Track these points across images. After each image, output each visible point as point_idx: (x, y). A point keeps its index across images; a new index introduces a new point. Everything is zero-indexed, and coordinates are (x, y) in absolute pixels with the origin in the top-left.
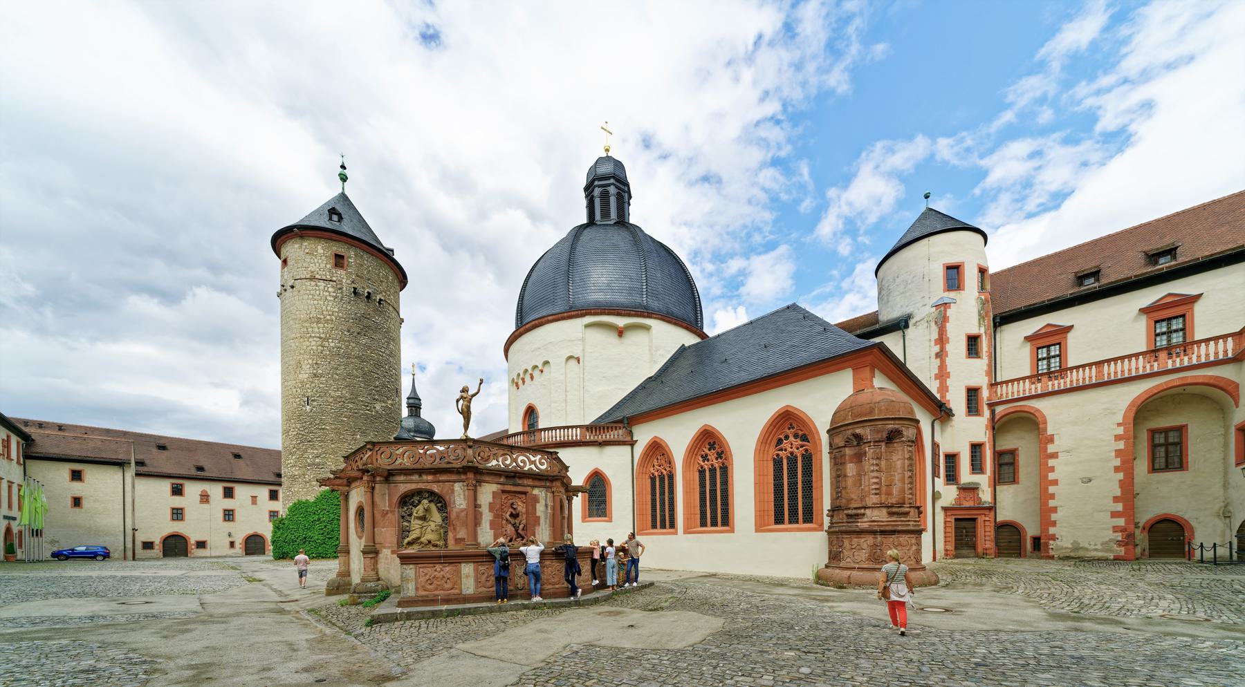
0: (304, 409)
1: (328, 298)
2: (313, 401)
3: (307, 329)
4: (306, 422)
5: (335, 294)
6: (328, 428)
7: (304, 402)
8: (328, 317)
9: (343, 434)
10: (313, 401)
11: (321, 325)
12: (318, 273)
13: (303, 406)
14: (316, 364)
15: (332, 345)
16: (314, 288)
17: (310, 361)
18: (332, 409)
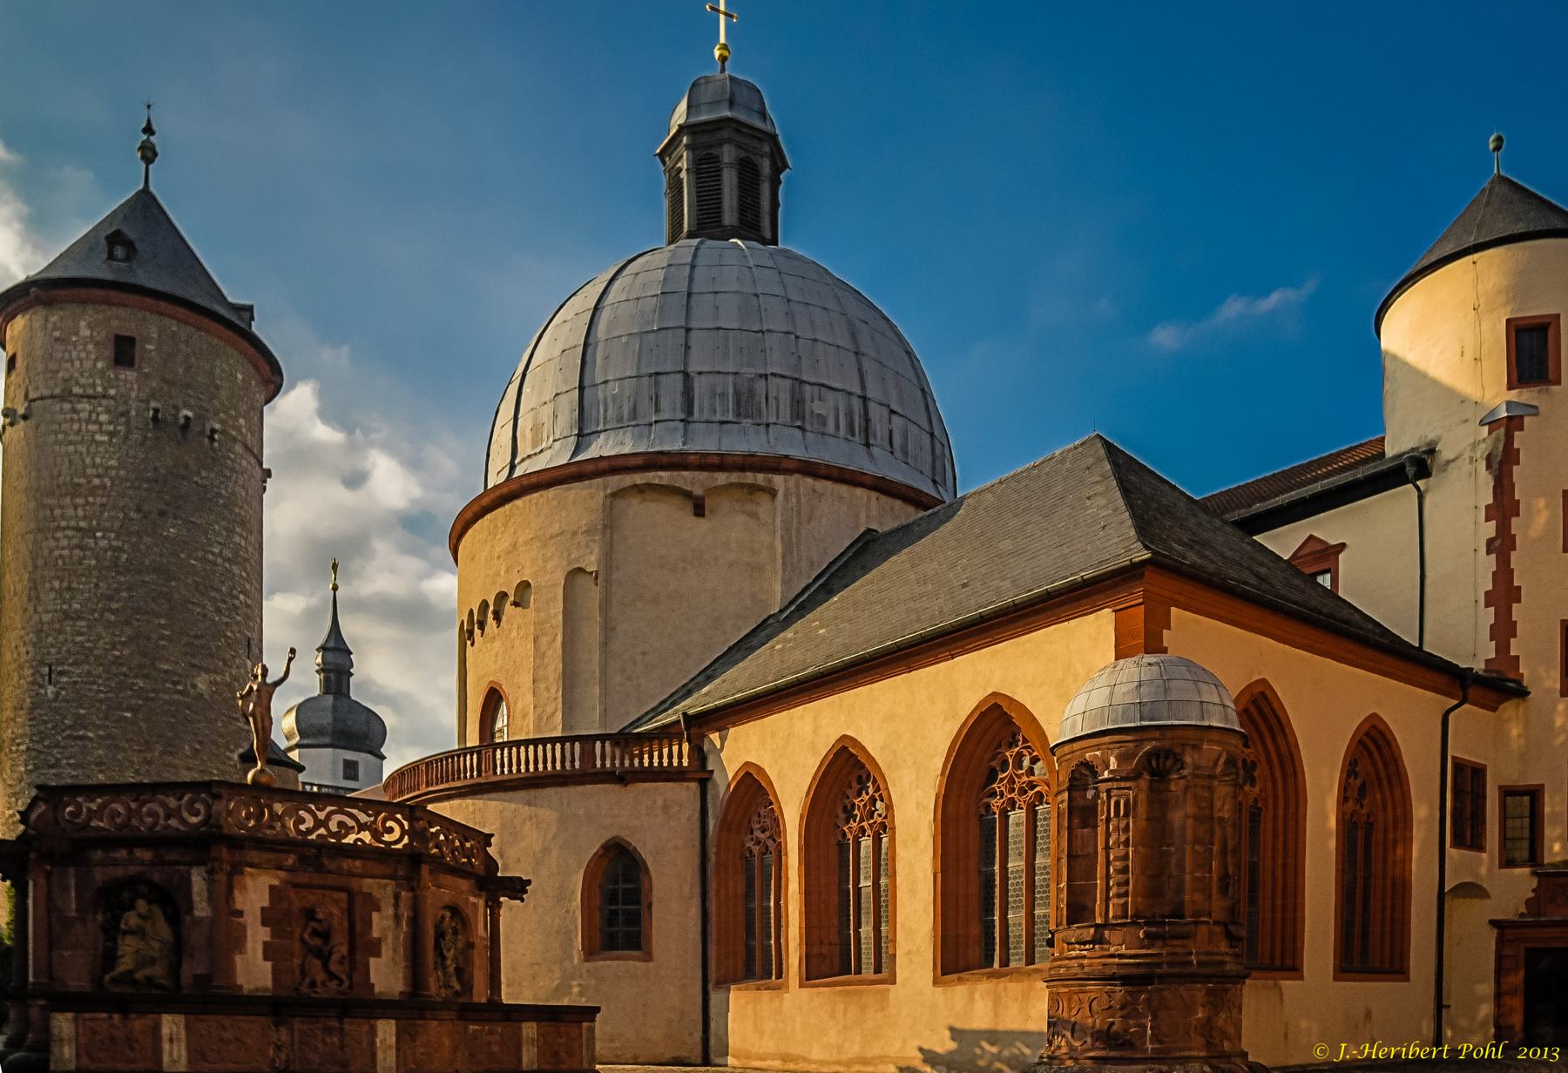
0: (42, 691)
1: (98, 437)
2: (61, 673)
3: (52, 510)
4: (45, 722)
5: (112, 428)
6: (91, 735)
7: (42, 676)
8: (96, 481)
9: (125, 750)
10: (61, 673)
11: (80, 501)
12: (77, 383)
13: (41, 686)
14: (69, 589)
15: (103, 543)
16: (68, 416)
17: (56, 584)
18: (101, 691)
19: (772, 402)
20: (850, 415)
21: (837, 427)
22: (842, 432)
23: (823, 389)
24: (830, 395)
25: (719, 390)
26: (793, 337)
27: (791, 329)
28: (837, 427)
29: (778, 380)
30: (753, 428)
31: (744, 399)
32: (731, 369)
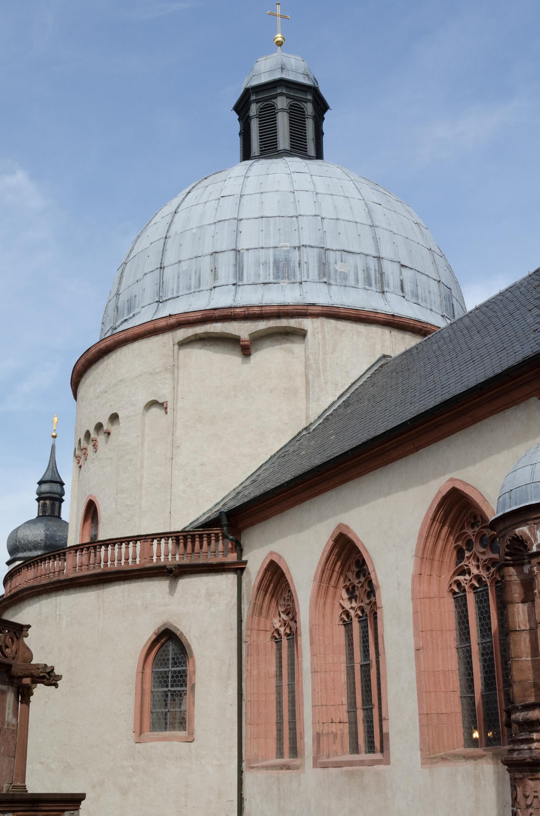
19: (304, 265)
20: (367, 270)
21: (357, 281)
22: (361, 285)
23: (343, 253)
24: (351, 259)
25: (262, 260)
26: (319, 218)
27: (317, 213)
28: (357, 281)
29: (308, 249)
30: (289, 286)
31: (281, 265)
32: (272, 245)
